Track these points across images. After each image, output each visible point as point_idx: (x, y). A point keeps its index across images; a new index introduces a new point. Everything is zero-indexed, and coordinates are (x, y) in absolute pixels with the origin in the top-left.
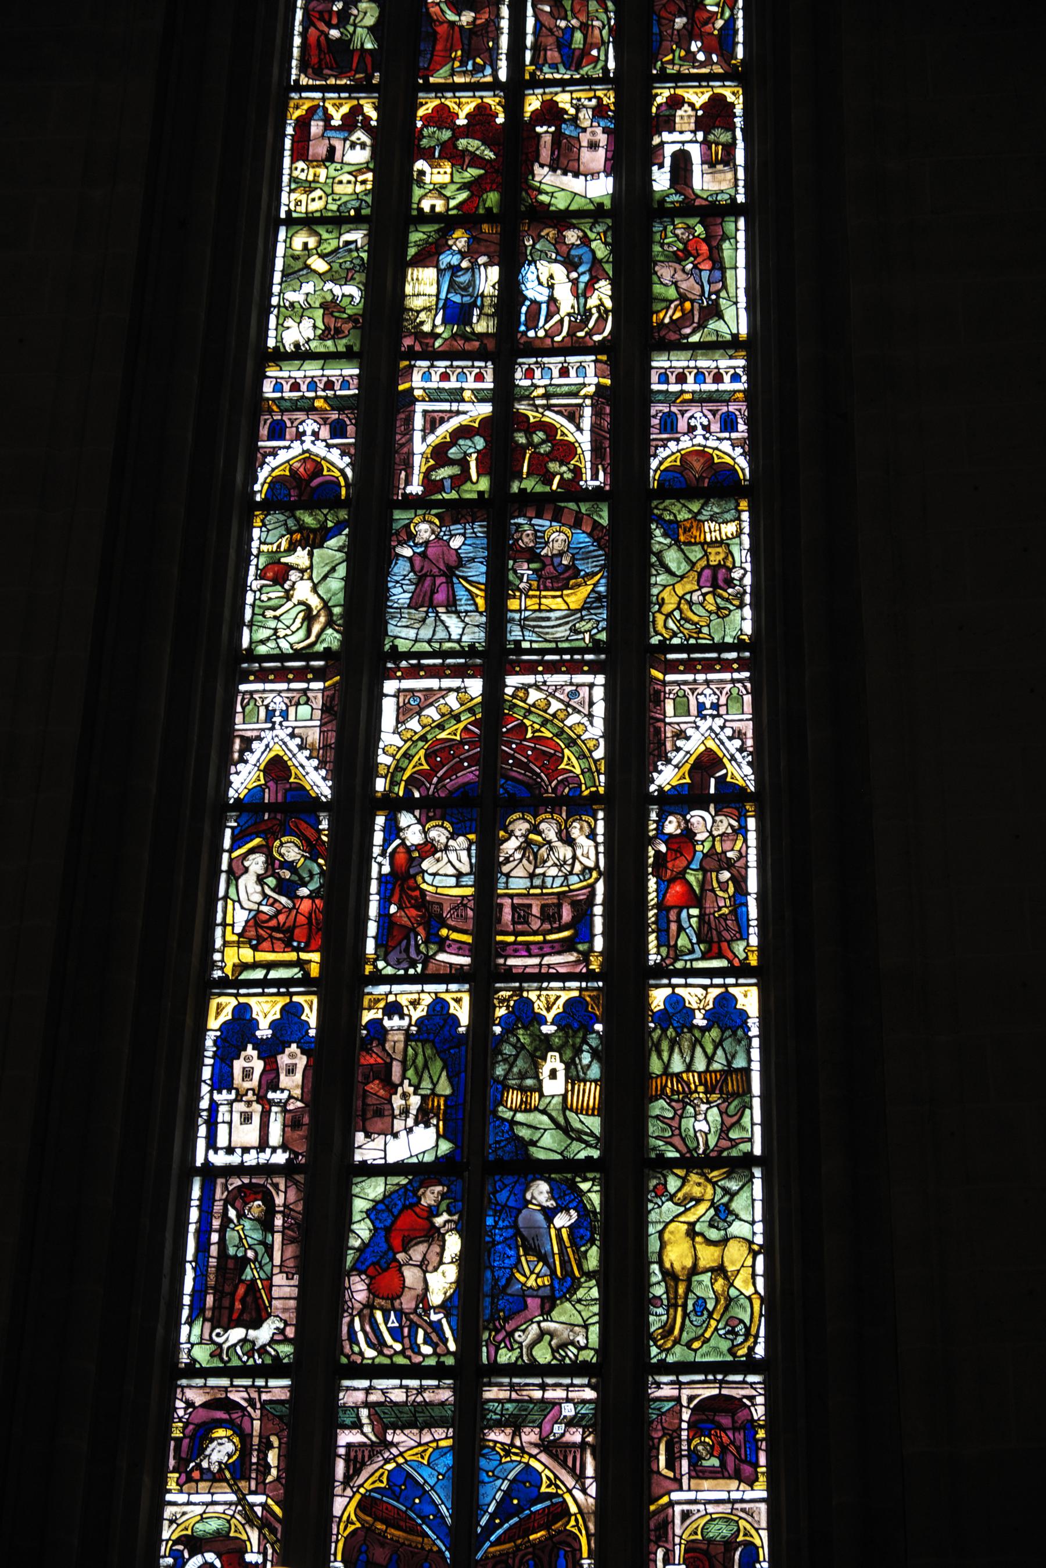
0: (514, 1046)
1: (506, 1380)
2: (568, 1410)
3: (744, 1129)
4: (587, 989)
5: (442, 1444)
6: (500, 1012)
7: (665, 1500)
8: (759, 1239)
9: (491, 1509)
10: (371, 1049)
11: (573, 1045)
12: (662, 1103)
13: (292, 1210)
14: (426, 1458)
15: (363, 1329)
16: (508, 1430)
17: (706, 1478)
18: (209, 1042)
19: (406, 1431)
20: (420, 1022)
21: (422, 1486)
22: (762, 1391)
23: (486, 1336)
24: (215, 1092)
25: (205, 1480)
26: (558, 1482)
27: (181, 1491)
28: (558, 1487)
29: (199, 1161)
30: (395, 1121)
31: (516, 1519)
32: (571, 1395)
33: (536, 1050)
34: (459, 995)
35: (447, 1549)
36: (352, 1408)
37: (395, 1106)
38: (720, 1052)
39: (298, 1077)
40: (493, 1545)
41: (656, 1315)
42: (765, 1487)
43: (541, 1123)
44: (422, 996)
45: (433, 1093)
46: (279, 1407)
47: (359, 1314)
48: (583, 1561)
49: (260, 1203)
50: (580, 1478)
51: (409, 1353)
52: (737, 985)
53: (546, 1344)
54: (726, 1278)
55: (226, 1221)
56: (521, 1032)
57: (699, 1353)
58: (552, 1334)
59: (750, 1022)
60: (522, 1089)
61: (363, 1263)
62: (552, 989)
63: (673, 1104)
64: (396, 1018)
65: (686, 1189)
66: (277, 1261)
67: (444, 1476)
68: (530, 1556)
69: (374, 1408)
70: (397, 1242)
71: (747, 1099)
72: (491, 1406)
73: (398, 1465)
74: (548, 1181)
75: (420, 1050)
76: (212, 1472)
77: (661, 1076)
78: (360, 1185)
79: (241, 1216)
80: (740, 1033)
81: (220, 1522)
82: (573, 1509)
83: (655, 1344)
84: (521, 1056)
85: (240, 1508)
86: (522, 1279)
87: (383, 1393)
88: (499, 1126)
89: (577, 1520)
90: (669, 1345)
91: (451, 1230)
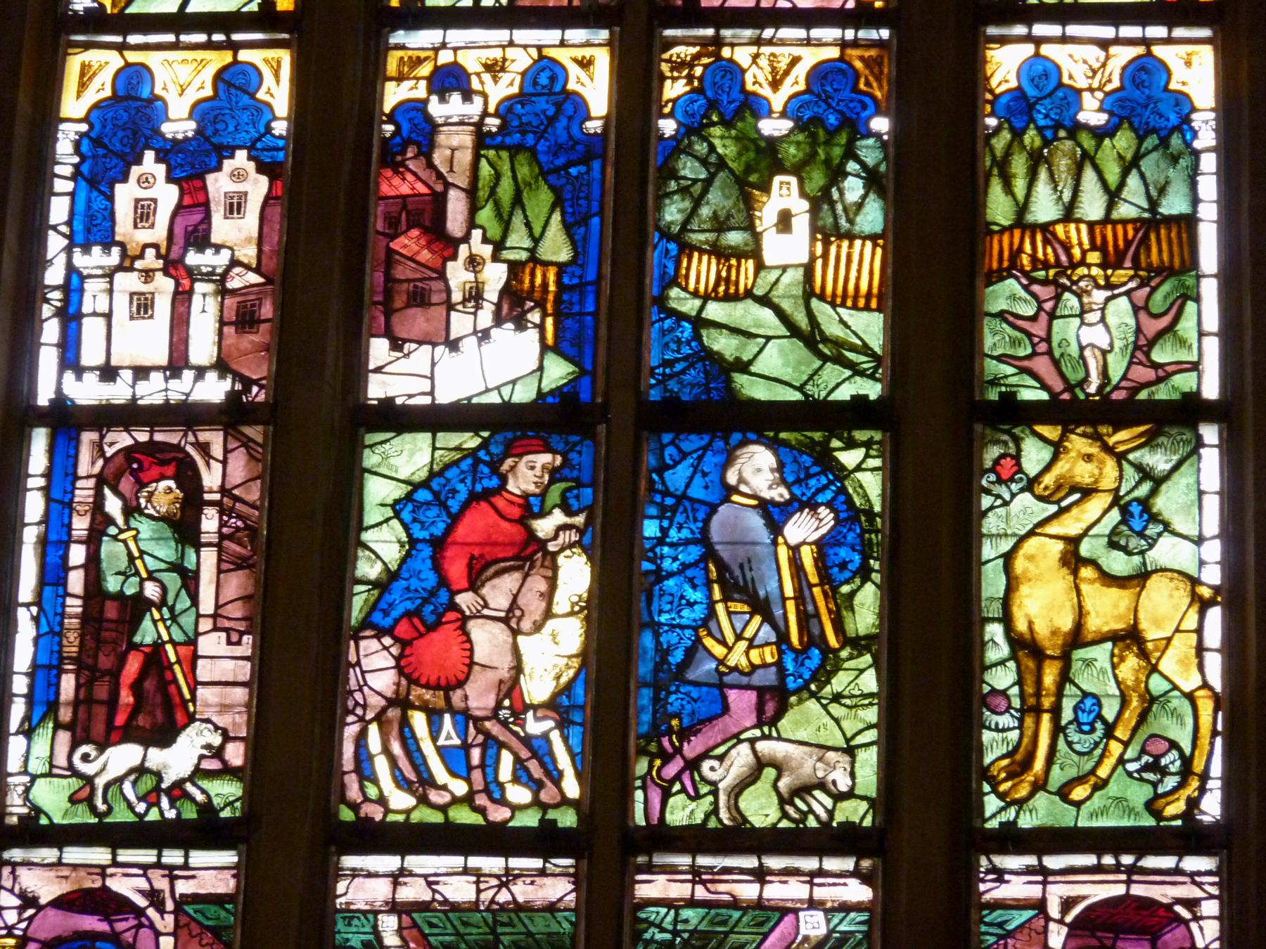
0: (704, 162)
1: (684, 860)
3: (1182, 342)
4: (855, 43)
6: (674, 89)
8: (1213, 575)
10: (402, 164)
11: (827, 162)
12: (1011, 285)
13: (237, 499)
15: (386, 751)
18: (64, 147)
20: (506, 110)
22: (1214, 891)
23: (641, 767)
24: (77, 250)
29: (44, 397)
30: (453, 314)
32: (819, 893)
33: (749, 169)
34: (587, 52)
36: (364, 912)
37: (452, 284)
38: (1133, 181)
39: (250, 221)
41: (997, 730)
43: (759, 326)
44: (510, 53)
45: (534, 259)
46: (212, 910)
47: (380, 718)
49: (171, 483)
51: (481, 800)
52: (1169, 41)
53: (768, 786)
54: (1144, 654)
55: (100, 521)
56: (717, 131)
57: (1085, 808)
58: (779, 768)
59: (1198, 119)
60: (719, 252)
61: (386, 613)
62: (783, 43)
63: (1036, 288)
64: (456, 98)
65: (1061, 468)
66: (207, 606)
69: (408, 913)
70: (457, 570)
71: (1190, 281)
72: (652, 913)
74: (774, 445)
75: (505, 168)
77: (1010, 229)
78: (379, 449)
79: (131, 510)
80: (1176, 141)
83: (995, 790)
84: (717, 183)
86: (719, 651)
87: (429, 884)
88: (671, 330)
90: (1023, 792)
91: (571, 546)
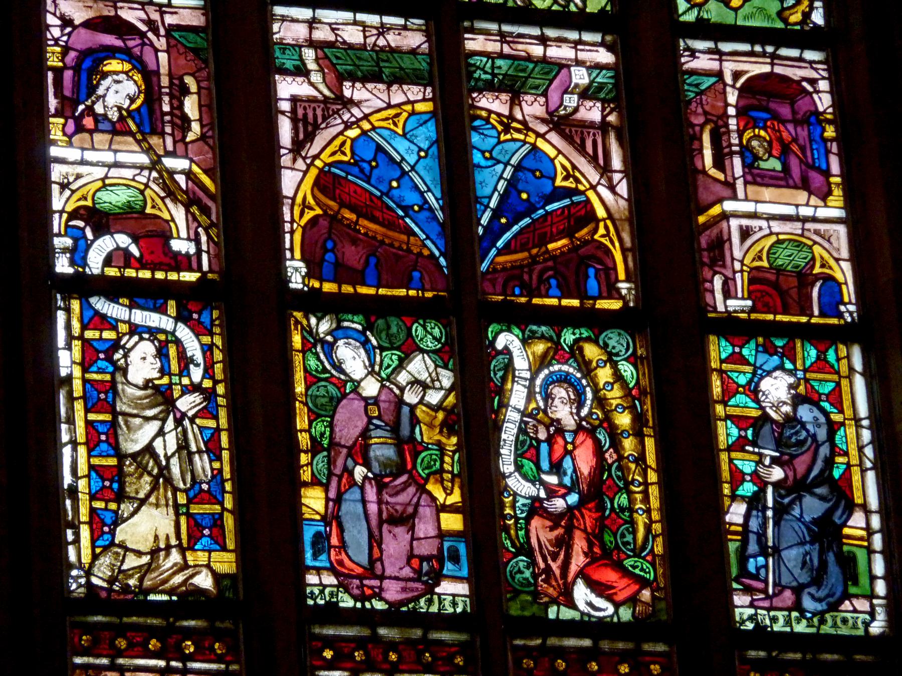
1: (494, 27)
2: (580, 77)
5: (420, 107)
7: (716, 210)
9: (493, 203)
14: (401, 125)
16: (505, 97)
17: (767, 185)
19: (370, 86)
21: (399, 164)
25: (103, 131)
26: (577, 174)
27: (70, 144)
28: (577, 181)
31: (527, 221)
32: (582, 56)
35: (442, 254)
36: (293, 46)
40: (500, 253)
42: (841, 204)
46: (191, 36)
48: (621, 285)
50: (605, 170)
67: (426, 152)
68: (551, 273)
69: (322, 49)
72: (476, 60)
73: (364, 133)
76: (110, 121)
81: (131, 192)
82: (601, 213)
85: (155, 174)
87: (333, 30)
89: (606, 228)
